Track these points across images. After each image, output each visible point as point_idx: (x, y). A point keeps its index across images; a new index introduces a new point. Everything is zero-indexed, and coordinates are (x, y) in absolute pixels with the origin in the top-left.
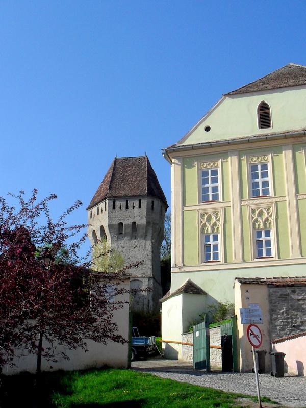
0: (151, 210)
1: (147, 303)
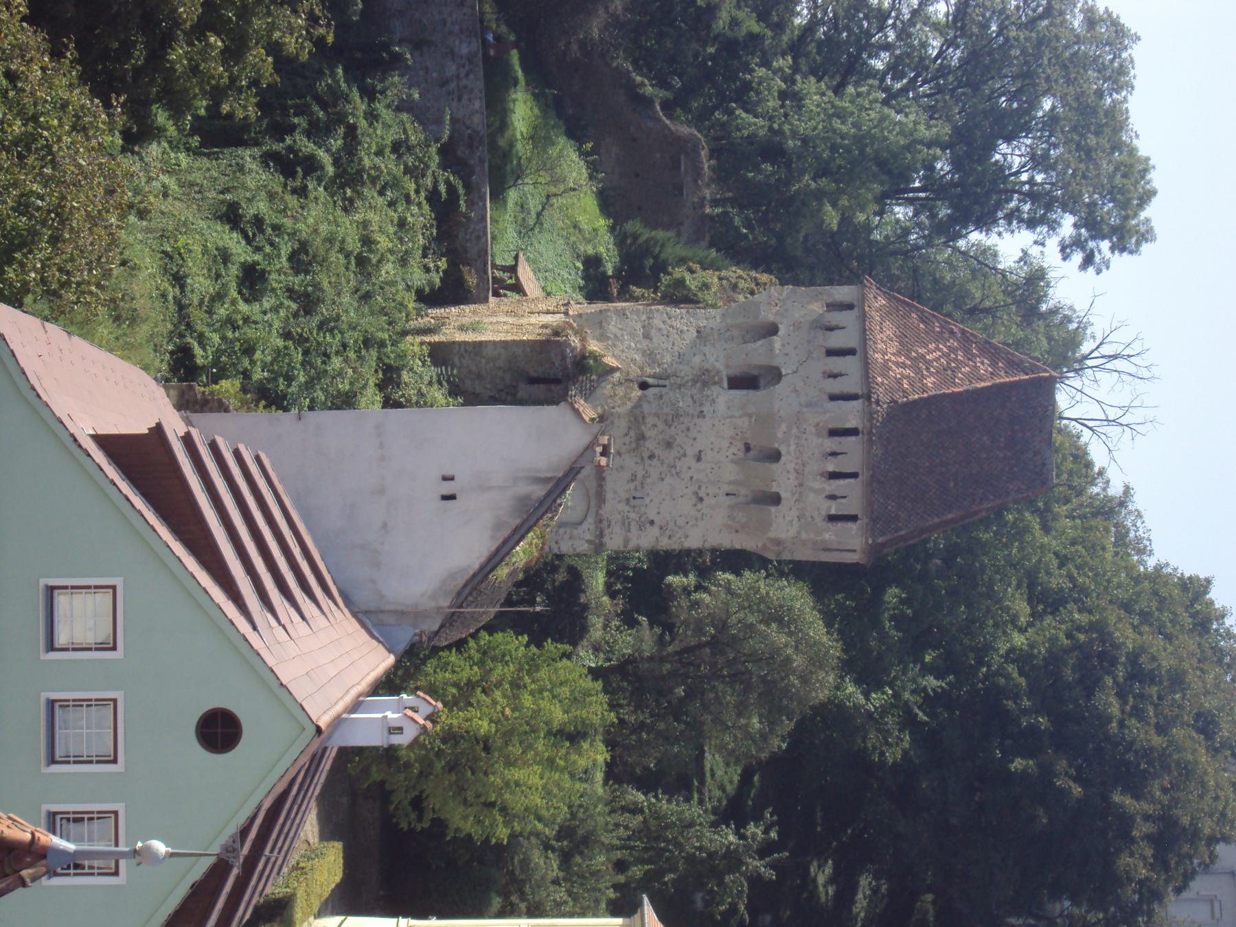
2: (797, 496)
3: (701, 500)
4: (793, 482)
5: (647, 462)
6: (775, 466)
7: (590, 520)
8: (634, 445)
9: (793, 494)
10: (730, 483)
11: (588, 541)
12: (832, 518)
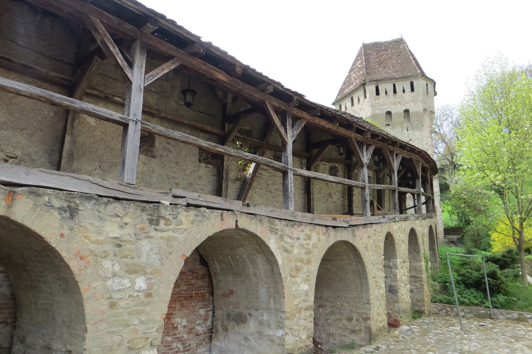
0: (426, 95)
2: (405, 104)
4: (399, 105)
6: (393, 112)
9: (404, 105)
10: (402, 129)
12: (412, 90)
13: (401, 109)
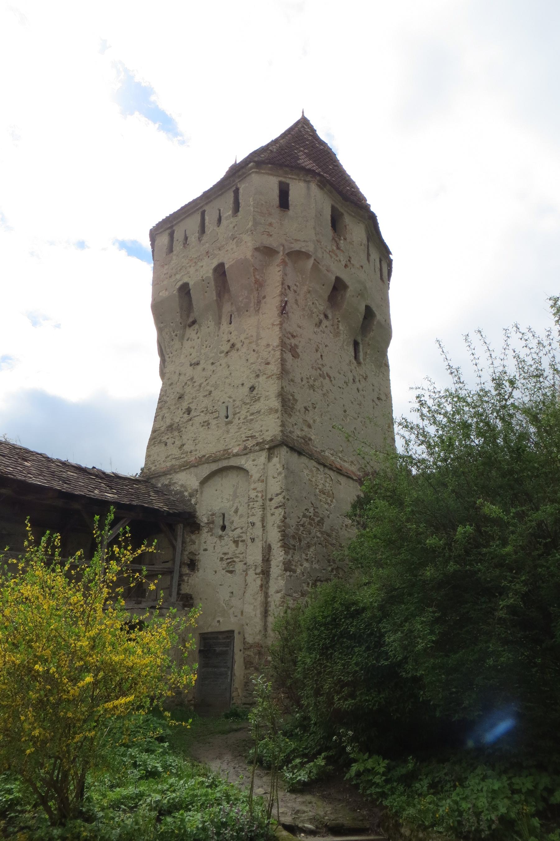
0: (276, 211)
1: (259, 558)
3: (233, 345)
5: (193, 413)
7: (241, 462)
8: (176, 433)
11: (269, 459)
13: (207, 269)
